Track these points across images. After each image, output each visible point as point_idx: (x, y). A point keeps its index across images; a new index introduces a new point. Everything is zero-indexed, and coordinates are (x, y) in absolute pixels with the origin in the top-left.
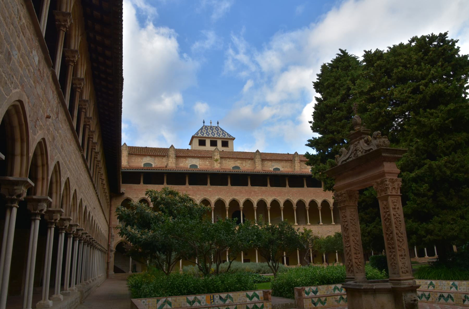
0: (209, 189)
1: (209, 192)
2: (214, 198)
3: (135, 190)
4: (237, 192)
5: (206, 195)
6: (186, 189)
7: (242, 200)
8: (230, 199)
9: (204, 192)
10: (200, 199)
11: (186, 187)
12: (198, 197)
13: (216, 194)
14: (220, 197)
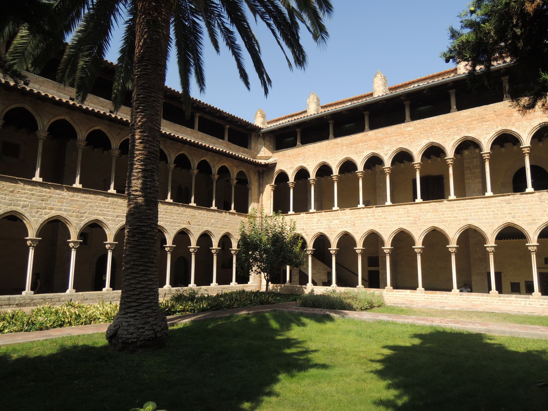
0: (409, 129)
1: (407, 136)
2: (418, 146)
3: (289, 156)
4: (474, 120)
5: (401, 142)
6: (364, 138)
7: (485, 138)
8: (455, 140)
9: (397, 137)
10: (390, 153)
11: (364, 136)
12: (385, 150)
13: (422, 136)
14: (432, 140)
